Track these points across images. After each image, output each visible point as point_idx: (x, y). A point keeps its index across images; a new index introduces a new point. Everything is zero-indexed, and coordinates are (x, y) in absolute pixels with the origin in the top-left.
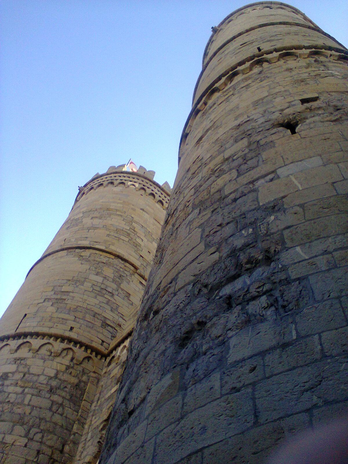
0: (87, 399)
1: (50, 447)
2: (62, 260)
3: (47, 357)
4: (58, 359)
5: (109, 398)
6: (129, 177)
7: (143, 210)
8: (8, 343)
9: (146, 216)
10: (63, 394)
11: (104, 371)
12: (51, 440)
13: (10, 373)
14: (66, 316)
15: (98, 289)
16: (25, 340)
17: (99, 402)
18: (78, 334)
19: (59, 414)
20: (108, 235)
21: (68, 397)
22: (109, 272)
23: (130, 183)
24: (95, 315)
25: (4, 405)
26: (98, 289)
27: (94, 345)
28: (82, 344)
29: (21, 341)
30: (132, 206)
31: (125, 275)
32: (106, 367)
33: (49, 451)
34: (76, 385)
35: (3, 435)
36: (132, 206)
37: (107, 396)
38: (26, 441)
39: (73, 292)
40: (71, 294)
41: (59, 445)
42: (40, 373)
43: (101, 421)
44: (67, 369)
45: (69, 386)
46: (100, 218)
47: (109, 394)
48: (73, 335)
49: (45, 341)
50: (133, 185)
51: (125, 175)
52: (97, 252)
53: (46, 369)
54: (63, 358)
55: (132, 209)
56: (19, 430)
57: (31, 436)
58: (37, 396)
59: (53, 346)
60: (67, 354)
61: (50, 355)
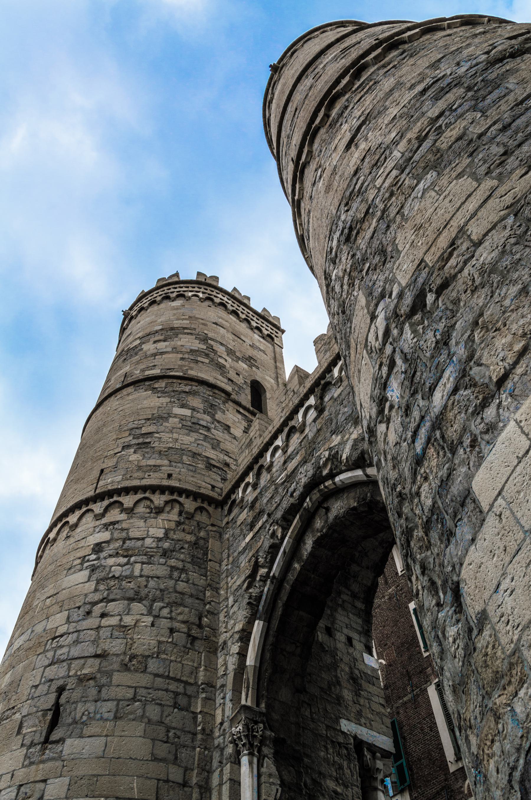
0: (213, 559)
1: (184, 622)
2: (131, 397)
4: (164, 516)
5: (245, 549)
7: (216, 323)
8: (88, 508)
9: (222, 330)
10: (182, 556)
11: (224, 522)
12: (184, 613)
13: (104, 542)
14: (159, 462)
15: (189, 424)
16: (112, 500)
17: (231, 559)
18: (180, 480)
19: (182, 581)
20: (182, 359)
21: (189, 560)
22: (196, 402)
24: (195, 455)
25: (109, 581)
26: (189, 424)
29: (106, 502)
30: (202, 321)
31: (217, 404)
32: (226, 516)
33: (184, 628)
34: (195, 544)
36: (202, 321)
37: (240, 549)
39: (158, 433)
40: (156, 435)
41: (194, 619)
43: (243, 578)
44: (177, 526)
45: (186, 546)
46: (165, 341)
47: (243, 544)
49: (139, 496)
52: (175, 381)
53: (150, 529)
55: (203, 324)
56: (137, 607)
57: (154, 613)
59: (151, 501)
60: (172, 508)
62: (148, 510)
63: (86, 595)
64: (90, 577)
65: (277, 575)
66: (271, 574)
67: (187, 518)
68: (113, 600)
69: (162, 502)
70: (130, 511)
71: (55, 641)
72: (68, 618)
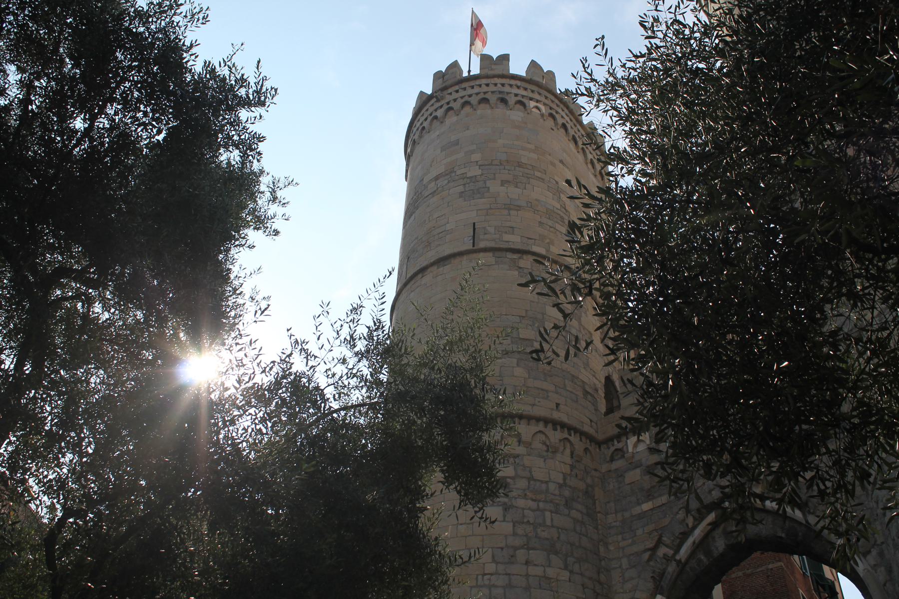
3: (545, 454)
4: (559, 456)
5: (642, 516)
6: (526, 89)
7: (561, 162)
13: (509, 477)
21: (585, 511)
23: (532, 104)
27: (587, 429)
28: (576, 430)
35: (542, 568)
38: (568, 574)
42: (547, 479)
47: (637, 510)
48: (565, 419)
50: (537, 107)
51: (519, 83)
54: (562, 453)
58: (556, 513)
59: (546, 436)
61: (547, 451)
62: (545, 448)
63: (506, 536)
64: (504, 516)
65: (683, 560)
66: (678, 557)
67: (578, 461)
68: (533, 549)
69: (557, 441)
70: (528, 445)
71: (486, 577)
72: (493, 557)
